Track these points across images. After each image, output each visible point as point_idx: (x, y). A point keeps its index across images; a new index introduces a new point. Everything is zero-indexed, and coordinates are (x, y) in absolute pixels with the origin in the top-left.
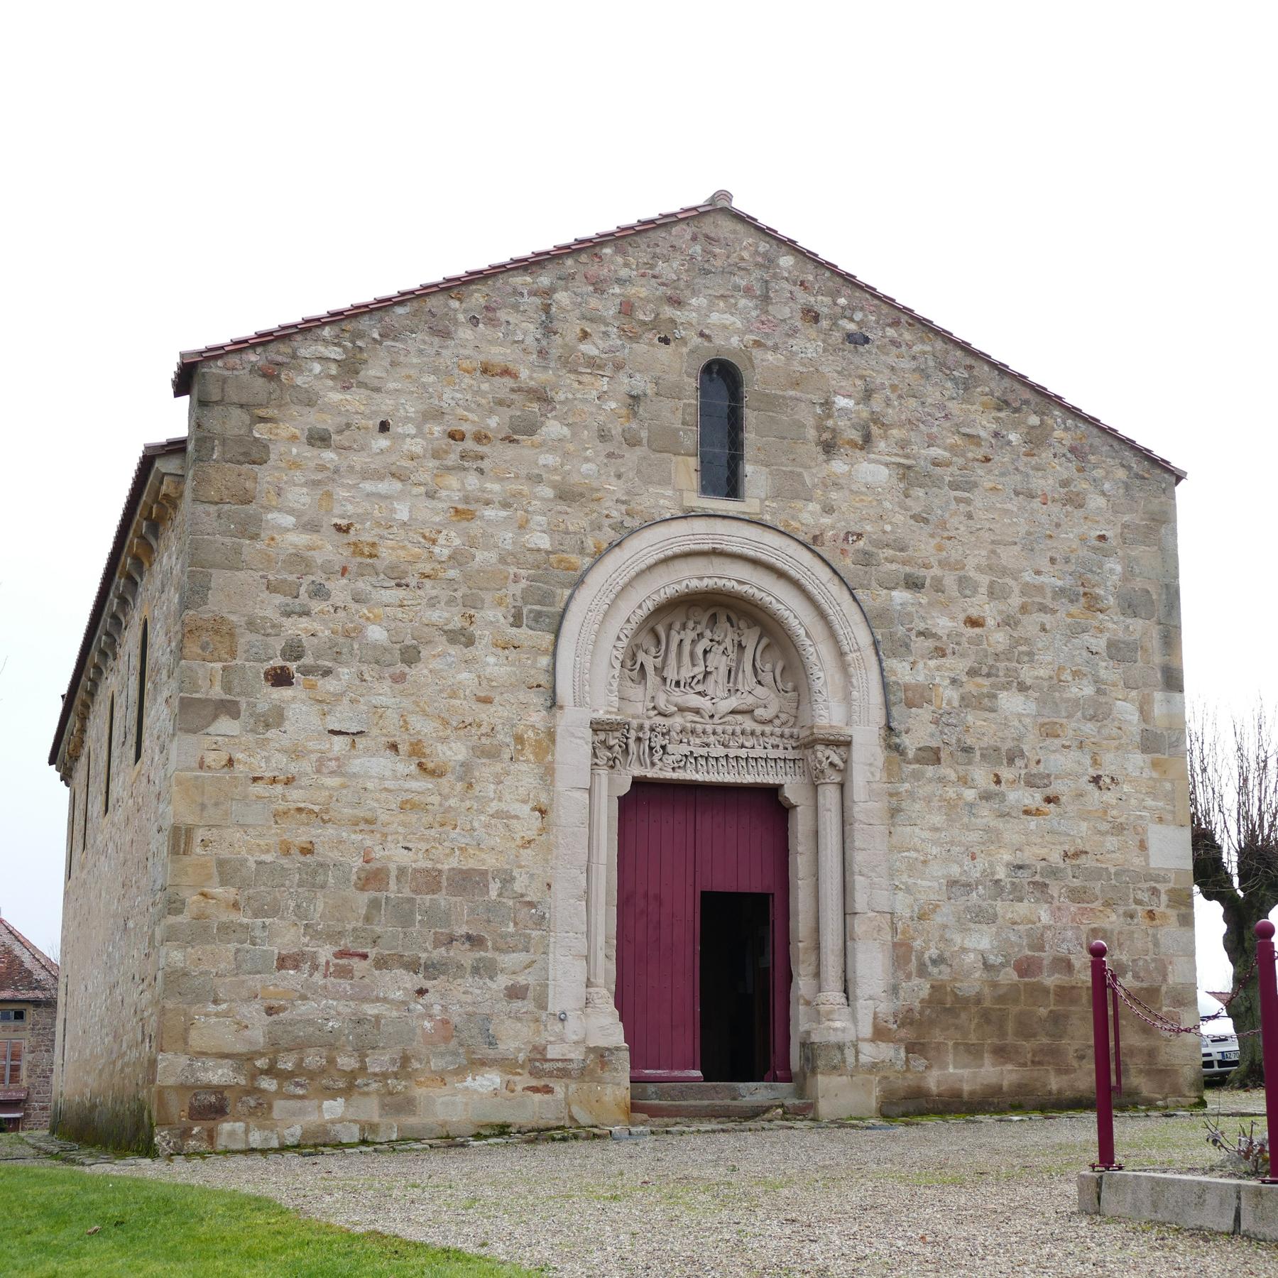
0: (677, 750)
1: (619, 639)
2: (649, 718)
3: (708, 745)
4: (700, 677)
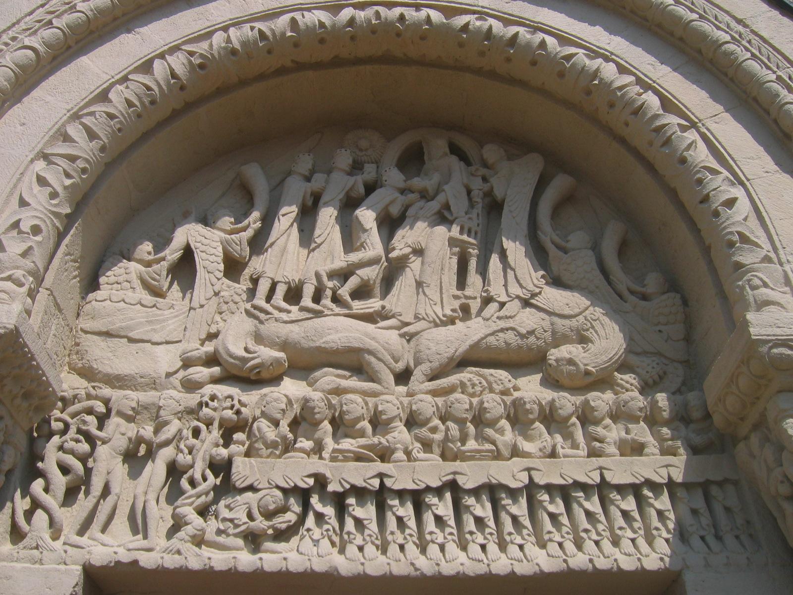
0: (269, 474)
1: (67, 138)
2: (191, 386)
3: (384, 455)
4: (371, 273)
